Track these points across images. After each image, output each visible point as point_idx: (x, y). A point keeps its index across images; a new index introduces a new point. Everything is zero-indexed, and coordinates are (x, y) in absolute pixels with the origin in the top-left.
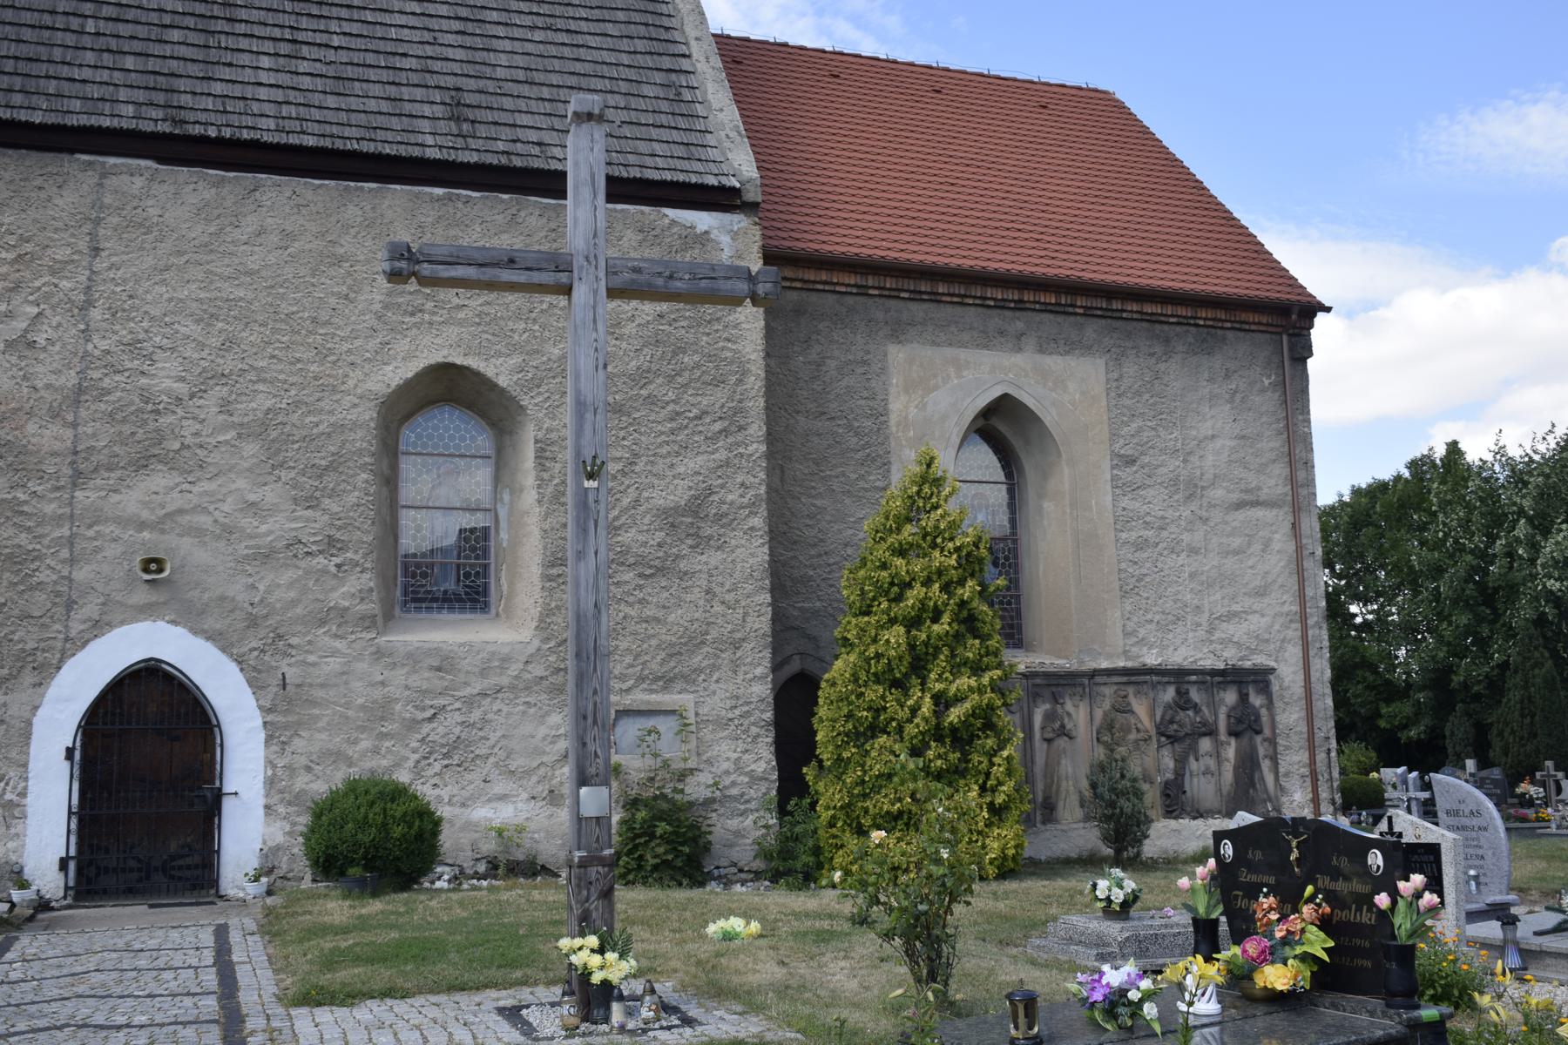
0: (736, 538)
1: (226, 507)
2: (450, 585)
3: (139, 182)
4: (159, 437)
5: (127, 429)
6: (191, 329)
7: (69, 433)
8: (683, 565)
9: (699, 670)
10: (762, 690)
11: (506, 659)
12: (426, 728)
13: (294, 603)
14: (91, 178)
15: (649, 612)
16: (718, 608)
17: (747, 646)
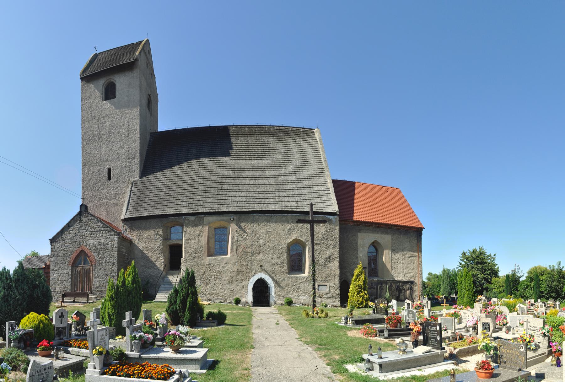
0: (335, 262)
1: (269, 258)
2: (297, 268)
3: (258, 217)
4: (261, 250)
5: (257, 249)
6: (264, 236)
7: (251, 250)
8: (327, 265)
9: (329, 280)
10: (338, 282)
11: (304, 278)
12: (294, 287)
13: (278, 270)
14: (252, 217)
15: (323, 272)
16: (332, 271)
17: (336, 276)
